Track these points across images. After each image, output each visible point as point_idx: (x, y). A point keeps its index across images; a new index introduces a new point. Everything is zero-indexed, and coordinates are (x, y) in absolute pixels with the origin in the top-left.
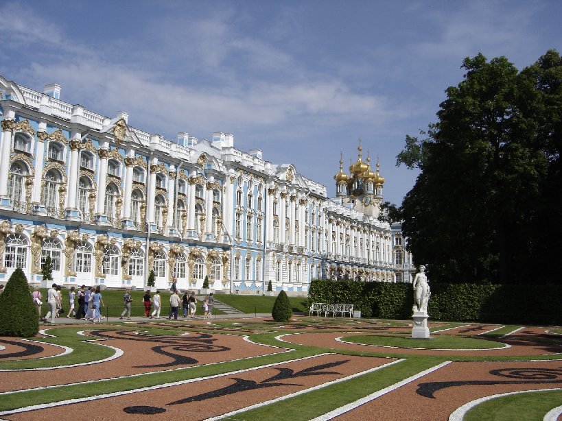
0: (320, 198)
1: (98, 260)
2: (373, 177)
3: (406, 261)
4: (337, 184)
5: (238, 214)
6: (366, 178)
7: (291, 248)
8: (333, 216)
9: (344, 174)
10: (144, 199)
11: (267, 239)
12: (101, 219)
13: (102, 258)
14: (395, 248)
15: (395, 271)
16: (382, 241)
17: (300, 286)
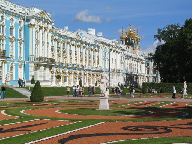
0: (123, 50)
1: (74, 78)
2: (136, 38)
3: (151, 72)
4: (121, 40)
5: (103, 60)
6: (134, 38)
7: (117, 70)
8: (128, 57)
9: (124, 36)
10: (54, 52)
11: (110, 68)
12: (74, 65)
13: (75, 78)
14: (146, 67)
15: (146, 77)
16: (142, 65)
17: (114, 84)
